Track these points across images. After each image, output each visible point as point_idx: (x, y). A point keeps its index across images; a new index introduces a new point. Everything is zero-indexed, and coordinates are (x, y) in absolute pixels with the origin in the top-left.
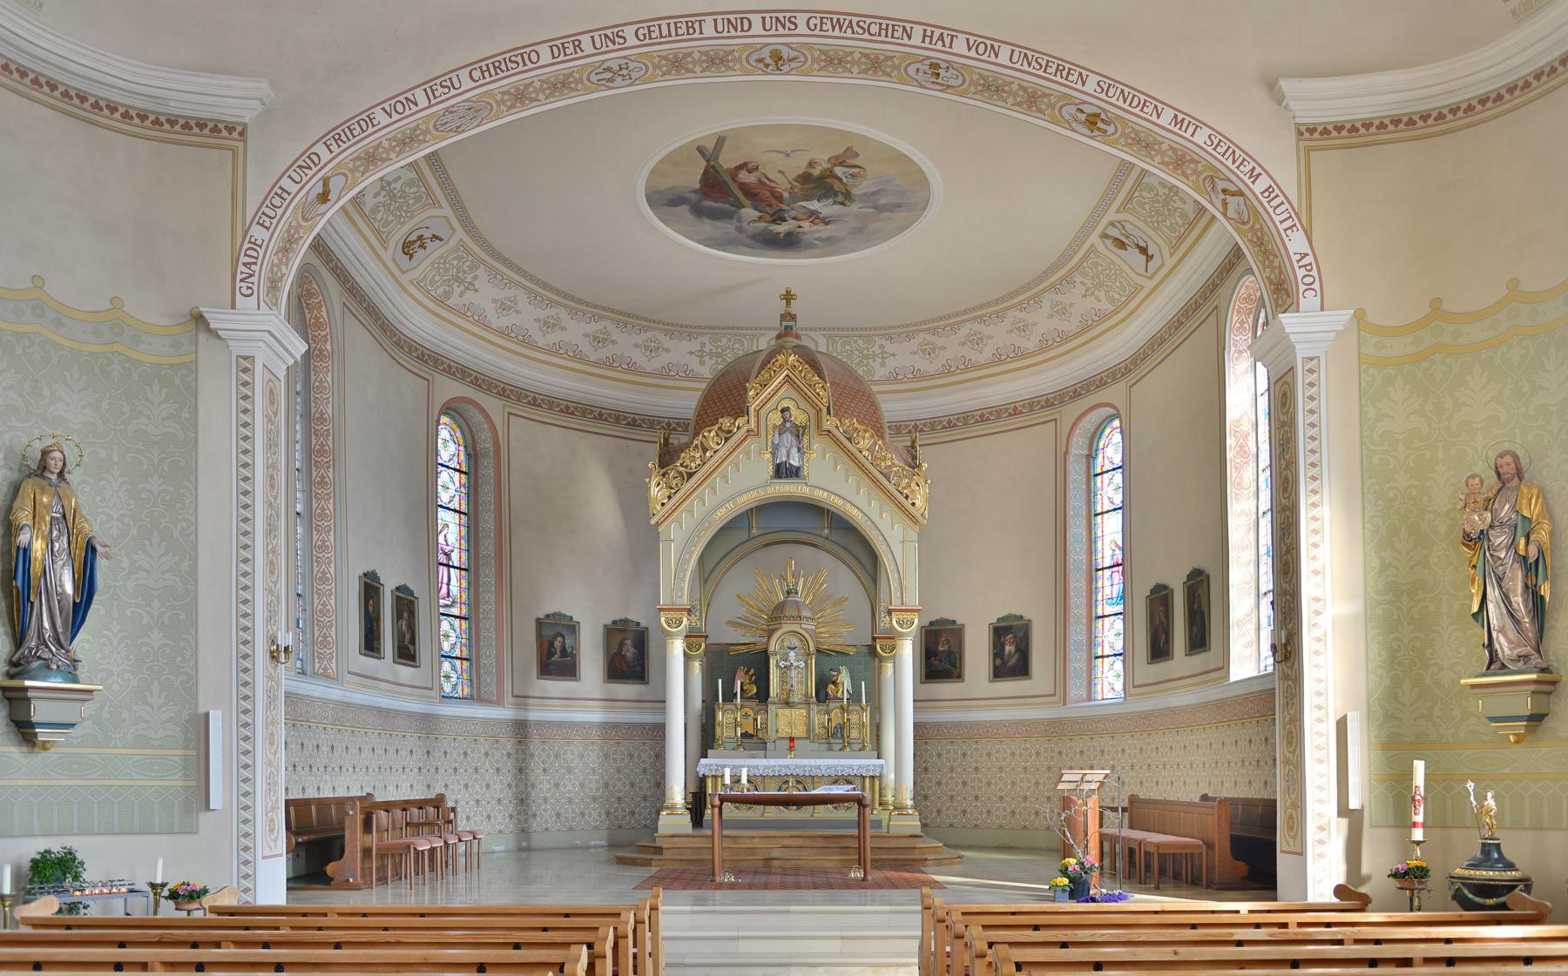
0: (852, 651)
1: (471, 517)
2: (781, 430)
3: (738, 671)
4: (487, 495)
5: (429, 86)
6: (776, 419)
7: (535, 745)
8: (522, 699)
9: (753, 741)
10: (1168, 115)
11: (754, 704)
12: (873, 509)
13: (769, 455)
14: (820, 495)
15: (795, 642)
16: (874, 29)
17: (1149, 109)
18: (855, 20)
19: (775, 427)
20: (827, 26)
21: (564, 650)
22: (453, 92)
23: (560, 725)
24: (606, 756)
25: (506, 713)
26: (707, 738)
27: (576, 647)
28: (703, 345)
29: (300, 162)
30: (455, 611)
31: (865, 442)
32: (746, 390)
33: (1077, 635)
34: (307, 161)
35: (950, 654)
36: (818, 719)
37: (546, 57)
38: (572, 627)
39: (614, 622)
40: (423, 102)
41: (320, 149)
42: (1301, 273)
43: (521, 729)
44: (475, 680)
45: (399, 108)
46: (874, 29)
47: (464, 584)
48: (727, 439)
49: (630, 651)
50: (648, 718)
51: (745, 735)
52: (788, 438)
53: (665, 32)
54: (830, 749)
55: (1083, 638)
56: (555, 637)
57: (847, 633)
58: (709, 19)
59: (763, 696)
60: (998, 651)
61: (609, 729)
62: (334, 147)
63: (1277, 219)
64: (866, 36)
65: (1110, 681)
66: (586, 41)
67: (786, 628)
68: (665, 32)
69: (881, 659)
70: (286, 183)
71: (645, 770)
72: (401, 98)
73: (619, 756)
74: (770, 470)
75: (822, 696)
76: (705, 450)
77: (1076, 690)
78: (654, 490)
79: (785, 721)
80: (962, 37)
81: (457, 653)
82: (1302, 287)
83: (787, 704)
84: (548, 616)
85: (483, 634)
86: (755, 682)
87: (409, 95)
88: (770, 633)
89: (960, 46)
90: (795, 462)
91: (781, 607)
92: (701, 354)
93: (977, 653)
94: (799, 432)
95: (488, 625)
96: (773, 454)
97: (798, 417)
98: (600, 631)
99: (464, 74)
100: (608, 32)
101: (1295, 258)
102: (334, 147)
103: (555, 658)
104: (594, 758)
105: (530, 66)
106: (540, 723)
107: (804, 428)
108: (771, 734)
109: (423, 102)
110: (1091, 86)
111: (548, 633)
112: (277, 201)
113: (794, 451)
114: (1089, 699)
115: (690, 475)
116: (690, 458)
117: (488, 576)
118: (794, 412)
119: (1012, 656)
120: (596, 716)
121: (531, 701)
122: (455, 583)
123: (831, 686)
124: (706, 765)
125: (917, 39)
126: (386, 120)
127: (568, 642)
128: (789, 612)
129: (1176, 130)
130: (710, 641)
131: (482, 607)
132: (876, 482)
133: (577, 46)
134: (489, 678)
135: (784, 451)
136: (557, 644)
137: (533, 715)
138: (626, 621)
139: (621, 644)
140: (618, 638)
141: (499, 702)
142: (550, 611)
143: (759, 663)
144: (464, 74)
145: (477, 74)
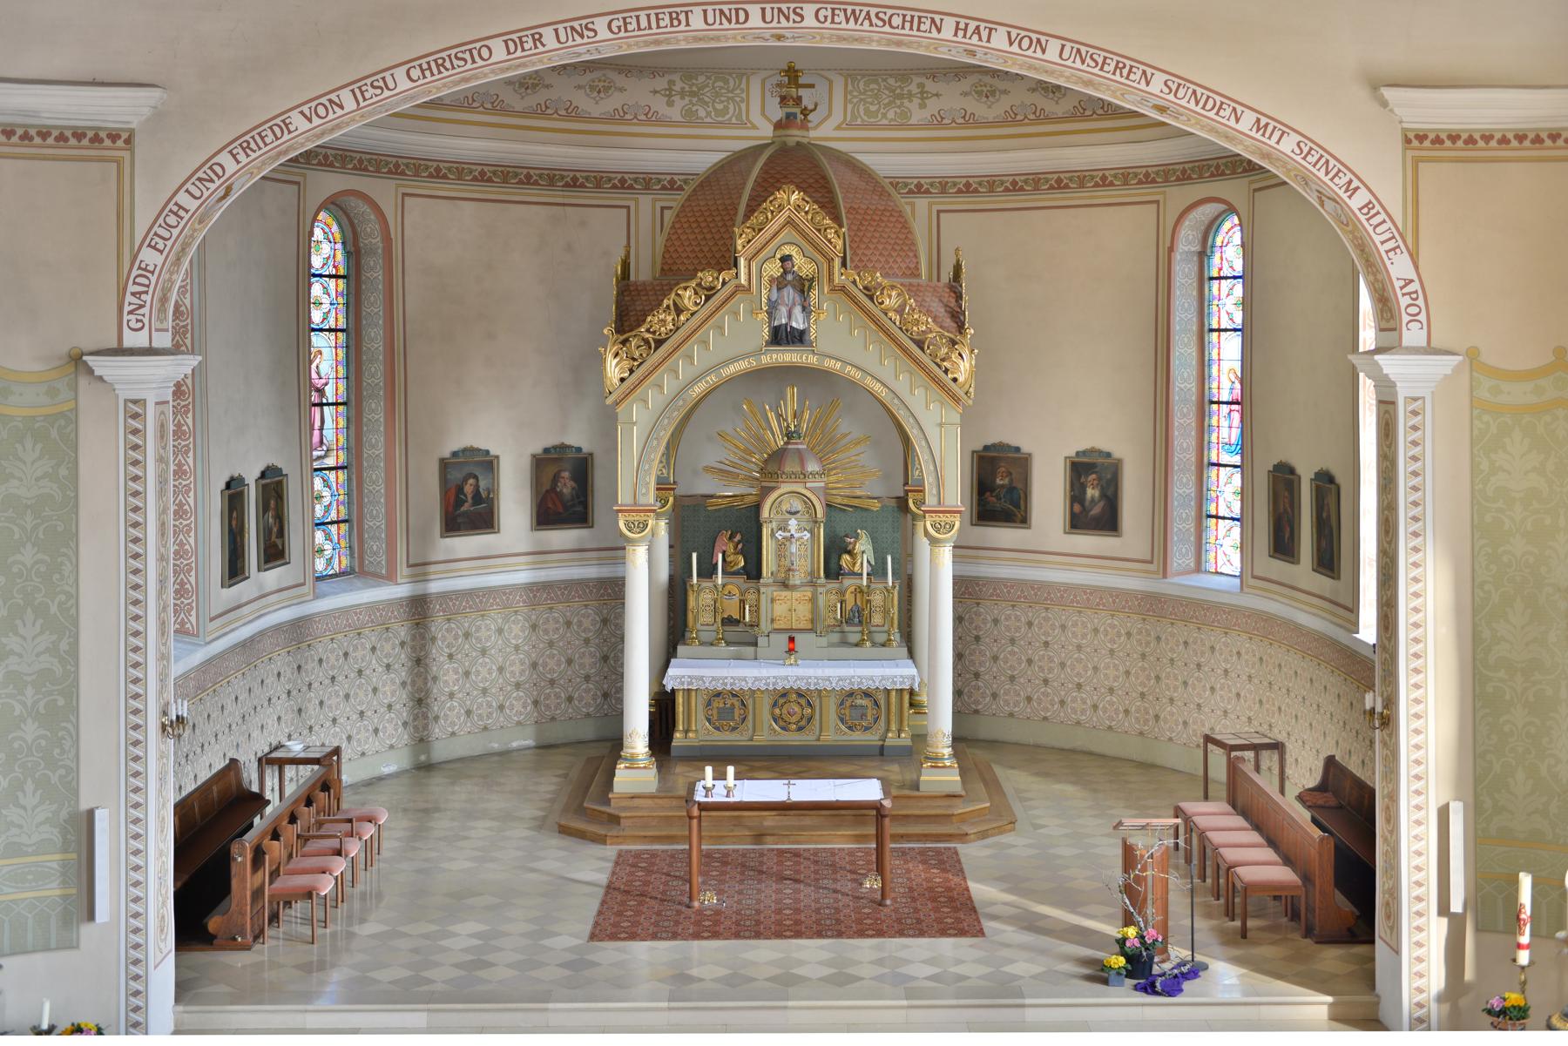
0: (876, 506)
1: (353, 335)
2: (780, 283)
3: (719, 534)
4: (374, 306)
5: (356, 86)
6: (774, 269)
7: (438, 626)
8: (420, 569)
9: (740, 633)
10: (1248, 119)
11: (740, 580)
12: (902, 383)
13: (764, 316)
14: (831, 364)
15: (797, 505)
16: (897, 21)
17: (1227, 112)
18: (873, 11)
19: (772, 280)
20: (841, 18)
21: (477, 494)
22: (387, 93)
23: (470, 593)
24: (534, 627)
25: (400, 590)
26: (674, 633)
27: (493, 490)
28: (671, 83)
29: (200, 174)
30: (330, 462)
31: (891, 301)
32: (732, 238)
33: (1182, 486)
34: (207, 171)
35: (1011, 489)
36: (827, 593)
37: (499, 53)
38: (488, 463)
39: (546, 450)
40: (350, 104)
41: (225, 158)
42: (1404, 301)
43: (419, 608)
44: (357, 548)
45: (321, 111)
46: (897, 21)
47: (342, 423)
48: (708, 298)
49: (567, 487)
50: (591, 572)
51: (729, 621)
52: (790, 294)
53: (644, 23)
54: (844, 643)
55: (1191, 490)
56: (465, 480)
57: (869, 481)
58: (698, 11)
59: (753, 571)
60: (1076, 495)
61: (536, 591)
62: (242, 157)
63: (1377, 239)
64: (887, 28)
65: (1226, 549)
66: (548, 33)
67: (785, 488)
68: (644, 23)
69: (915, 517)
70: (182, 198)
71: (587, 641)
72: (324, 100)
73: (551, 625)
74: (766, 333)
75: (833, 571)
76: (679, 311)
77: (1180, 556)
78: (613, 369)
79: (784, 607)
80: (1002, 30)
81: (333, 516)
82: (1405, 318)
83: (785, 585)
84: (455, 454)
85: (367, 487)
86: (742, 552)
87: (333, 97)
88: (765, 492)
89: (999, 40)
90: (798, 323)
91: (778, 456)
92: (669, 93)
93: (1048, 494)
94: (803, 286)
95: (375, 479)
96: (770, 314)
97: (804, 267)
98: (526, 463)
99: (400, 73)
100: (576, 24)
101: (1398, 284)
102: (242, 157)
103: (465, 508)
104: (517, 631)
105: (481, 63)
106: (445, 596)
107: (812, 280)
108: (765, 626)
109: (350, 104)
110: (1157, 85)
111: (455, 476)
112: (172, 220)
113: (797, 310)
114: (1199, 568)
115: (659, 343)
116: (662, 320)
117: (375, 411)
118: (798, 260)
119: (1095, 500)
120: (522, 576)
121: (432, 568)
122: (331, 423)
123: (846, 557)
124: (679, 674)
125: (948, 32)
126: (304, 125)
127: (483, 484)
128: (790, 466)
129: (1258, 136)
130: (681, 490)
131: (367, 452)
132: (904, 350)
133: (538, 39)
134: (376, 546)
135: (784, 310)
136: (468, 489)
137: (435, 587)
138: (563, 448)
139: (556, 478)
140: (551, 470)
141: (390, 577)
142: (455, 448)
143: (746, 526)
144: (400, 73)
145: (415, 73)
